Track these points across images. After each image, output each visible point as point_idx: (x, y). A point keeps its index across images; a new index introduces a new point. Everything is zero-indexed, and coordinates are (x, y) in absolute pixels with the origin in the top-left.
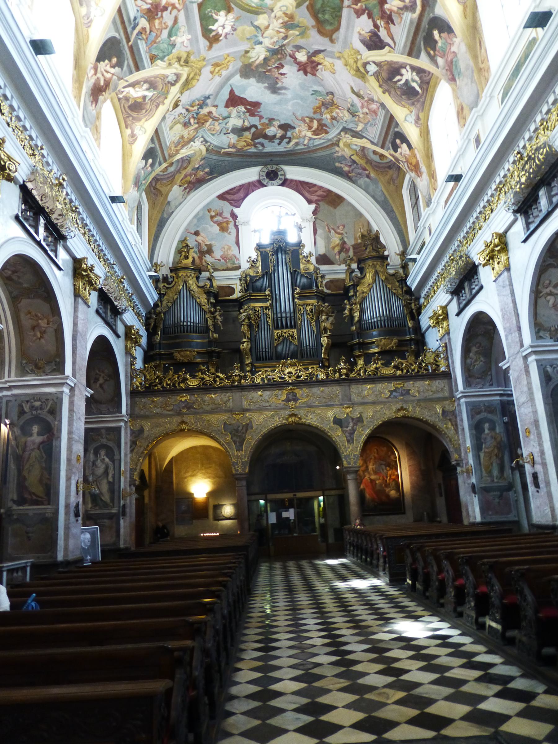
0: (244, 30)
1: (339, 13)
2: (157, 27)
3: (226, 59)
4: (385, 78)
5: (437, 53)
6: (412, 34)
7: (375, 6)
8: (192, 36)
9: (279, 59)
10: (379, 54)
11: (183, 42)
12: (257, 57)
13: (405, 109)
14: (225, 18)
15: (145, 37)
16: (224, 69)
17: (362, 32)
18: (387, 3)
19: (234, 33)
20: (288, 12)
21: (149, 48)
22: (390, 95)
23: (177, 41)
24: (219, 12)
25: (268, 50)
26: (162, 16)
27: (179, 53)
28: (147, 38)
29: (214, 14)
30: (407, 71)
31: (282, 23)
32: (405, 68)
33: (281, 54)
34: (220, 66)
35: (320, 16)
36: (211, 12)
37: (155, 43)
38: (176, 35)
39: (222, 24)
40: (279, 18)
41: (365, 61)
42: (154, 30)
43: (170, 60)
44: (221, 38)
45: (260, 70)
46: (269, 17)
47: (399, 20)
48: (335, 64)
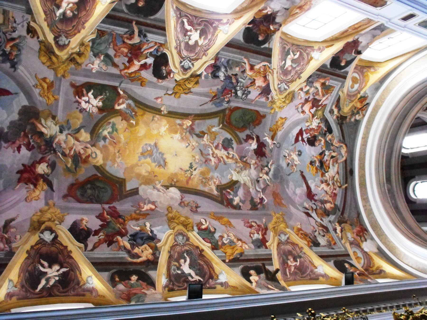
0: (78, 119)
1: (94, 201)
2: (122, 49)
3: (53, 97)
4: (41, 251)
5: (123, 282)
6: (113, 261)
7: (114, 229)
8: (94, 73)
9: (39, 147)
10: (71, 239)
11: (93, 65)
12: (45, 126)
13: (17, 279)
14: (95, 105)
15: (125, 36)
16: (42, 92)
17: (84, 222)
18: (122, 238)
19: (78, 110)
20: (90, 159)
21: (113, 34)
22: (27, 258)
23: (98, 59)
24: (102, 102)
25: (53, 138)
26: (126, 56)
27: (85, 57)
28: (122, 37)
29: (102, 97)
30: (58, 271)
31: (79, 153)
32: (62, 267)
33: (46, 149)
34: (48, 88)
35: (89, 186)
36: (106, 95)
37: (112, 42)
38: (103, 61)
39: (90, 101)
40: (85, 151)
41: (54, 229)
42: (123, 46)
43: (85, 47)
44: (77, 97)
45: (29, 127)
46: (88, 142)
47: (115, 249)
48: (38, 201)
